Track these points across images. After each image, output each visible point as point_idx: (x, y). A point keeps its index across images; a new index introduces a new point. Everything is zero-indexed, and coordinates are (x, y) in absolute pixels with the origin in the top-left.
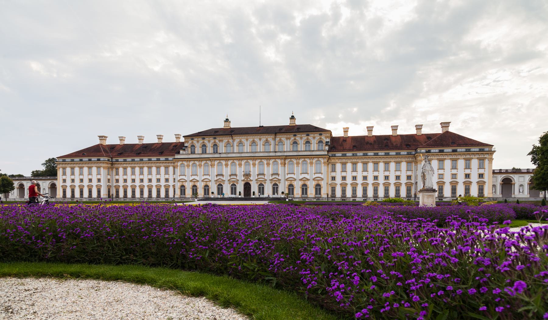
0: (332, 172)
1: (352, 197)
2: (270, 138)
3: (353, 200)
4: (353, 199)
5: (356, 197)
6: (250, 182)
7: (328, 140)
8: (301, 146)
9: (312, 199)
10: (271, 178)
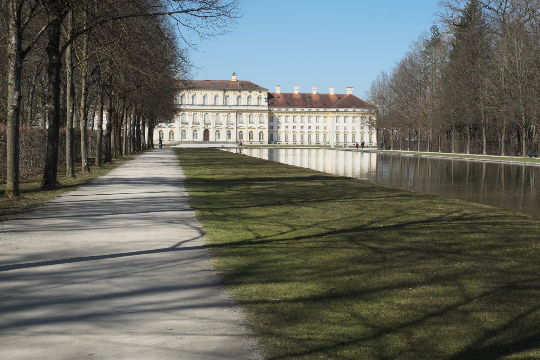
0: (271, 122)
1: (286, 141)
2: (220, 93)
3: (286, 144)
4: (287, 143)
5: (288, 142)
6: (209, 129)
7: (266, 97)
8: (244, 101)
9: (257, 143)
10: (226, 126)
